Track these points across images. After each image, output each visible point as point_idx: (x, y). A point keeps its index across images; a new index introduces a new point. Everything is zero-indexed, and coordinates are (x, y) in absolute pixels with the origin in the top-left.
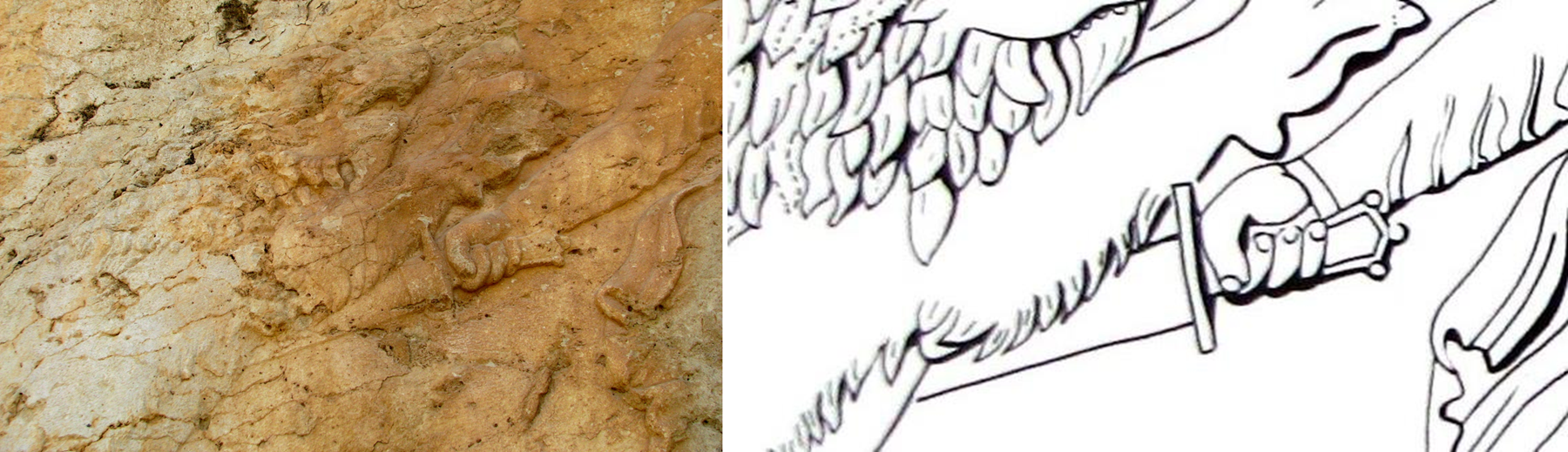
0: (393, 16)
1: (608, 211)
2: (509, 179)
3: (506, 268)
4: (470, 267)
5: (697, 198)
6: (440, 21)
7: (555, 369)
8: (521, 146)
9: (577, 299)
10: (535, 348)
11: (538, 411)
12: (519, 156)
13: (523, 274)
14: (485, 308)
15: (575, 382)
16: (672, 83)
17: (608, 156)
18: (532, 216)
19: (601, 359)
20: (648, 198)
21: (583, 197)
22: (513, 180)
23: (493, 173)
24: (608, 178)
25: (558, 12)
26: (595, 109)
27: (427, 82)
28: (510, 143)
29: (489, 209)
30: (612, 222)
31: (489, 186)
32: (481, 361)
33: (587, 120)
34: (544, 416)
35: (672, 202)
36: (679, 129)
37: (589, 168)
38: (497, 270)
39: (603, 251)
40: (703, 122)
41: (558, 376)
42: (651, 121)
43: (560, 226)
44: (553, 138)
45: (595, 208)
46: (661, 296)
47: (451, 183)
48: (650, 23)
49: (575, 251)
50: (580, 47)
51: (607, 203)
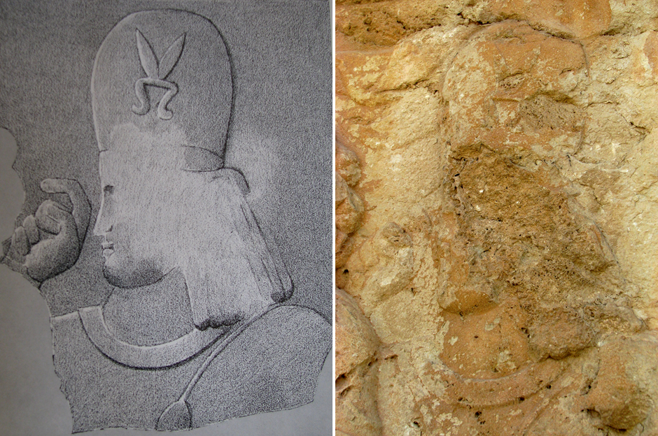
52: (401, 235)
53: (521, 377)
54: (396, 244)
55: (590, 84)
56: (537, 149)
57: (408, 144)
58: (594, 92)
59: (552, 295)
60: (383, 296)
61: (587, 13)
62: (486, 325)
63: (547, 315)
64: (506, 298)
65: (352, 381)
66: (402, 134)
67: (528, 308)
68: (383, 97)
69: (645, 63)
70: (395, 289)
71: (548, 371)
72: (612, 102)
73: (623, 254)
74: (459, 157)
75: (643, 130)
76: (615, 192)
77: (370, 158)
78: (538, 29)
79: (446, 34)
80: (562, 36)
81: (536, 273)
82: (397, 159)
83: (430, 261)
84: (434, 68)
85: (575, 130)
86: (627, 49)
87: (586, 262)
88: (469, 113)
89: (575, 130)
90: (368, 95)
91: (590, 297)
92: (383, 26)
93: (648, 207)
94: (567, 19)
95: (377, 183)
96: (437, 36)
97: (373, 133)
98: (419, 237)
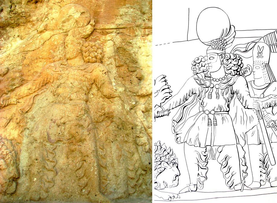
0: (7, 61)
1: (25, 96)
2: (13, 90)
3: (8, 104)
4: (2, 104)
5: (38, 95)
6: (12, 63)
7: (10, 120)
8: (15, 85)
9: (17, 110)
10: (9, 116)
11: (7, 125)
12: (14, 87)
13: (11, 105)
14: (4, 110)
15: (13, 122)
16: (40, 77)
17: (27, 88)
18: (14, 96)
19: (17, 119)
20: (31, 95)
21: (22, 94)
22: (13, 91)
23: (10, 89)
24: (26, 92)
25: (29, 63)
26: (29, 80)
27: (7, 73)
28: (14, 85)
29: (8, 95)
30: (25, 98)
31: (9, 91)
32: (2, 117)
33: (27, 81)
34: (7, 126)
35: (33, 96)
36: (39, 84)
37: (24, 90)
38: (7, 104)
39: (23, 103)
40: (42, 84)
41: (11, 121)
42: (35, 83)
43: (17, 98)
44: (20, 84)
45: (23, 96)
46: (27, 110)
47: (4, 90)
48: (41, 66)
49: (19, 102)
50: (30, 69)
51: (25, 95)
52: (109, 58)
53: (128, 74)
54: (109, 59)
55: (133, 41)
56: (128, 48)
57: (109, 47)
58: (134, 43)
59: (131, 65)
60: (108, 65)
61: (133, 33)
62: (123, 68)
63: (131, 67)
64: (125, 65)
65: (106, 73)
66: (109, 46)
67: (128, 66)
68: (105, 41)
69: (140, 40)
70: (109, 64)
71: (131, 73)
72: (136, 44)
73: (139, 61)
74: (118, 49)
75: (140, 48)
76: (137, 54)
77: (104, 48)
78: (127, 35)
79: (114, 34)
80: (130, 36)
81: (129, 62)
82: (108, 49)
83: (114, 61)
84: (112, 38)
85: (132, 47)
86: (137, 38)
87: (135, 62)
88: (119, 43)
89: (132, 47)
90: (104, 41)
91: (135, 65)
92: (105, 33)
93: (142, 56)
94: (130, 34)
95: (105, 52)
96: (112, 34)
97: (104, 45)
98: (112, 58)
